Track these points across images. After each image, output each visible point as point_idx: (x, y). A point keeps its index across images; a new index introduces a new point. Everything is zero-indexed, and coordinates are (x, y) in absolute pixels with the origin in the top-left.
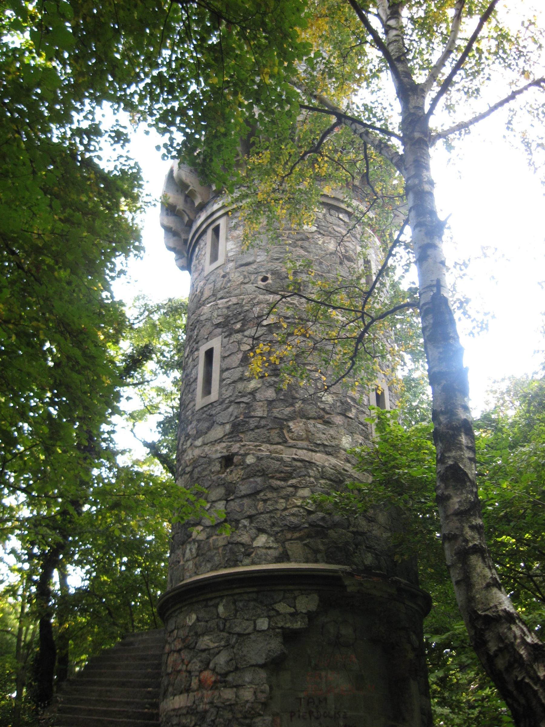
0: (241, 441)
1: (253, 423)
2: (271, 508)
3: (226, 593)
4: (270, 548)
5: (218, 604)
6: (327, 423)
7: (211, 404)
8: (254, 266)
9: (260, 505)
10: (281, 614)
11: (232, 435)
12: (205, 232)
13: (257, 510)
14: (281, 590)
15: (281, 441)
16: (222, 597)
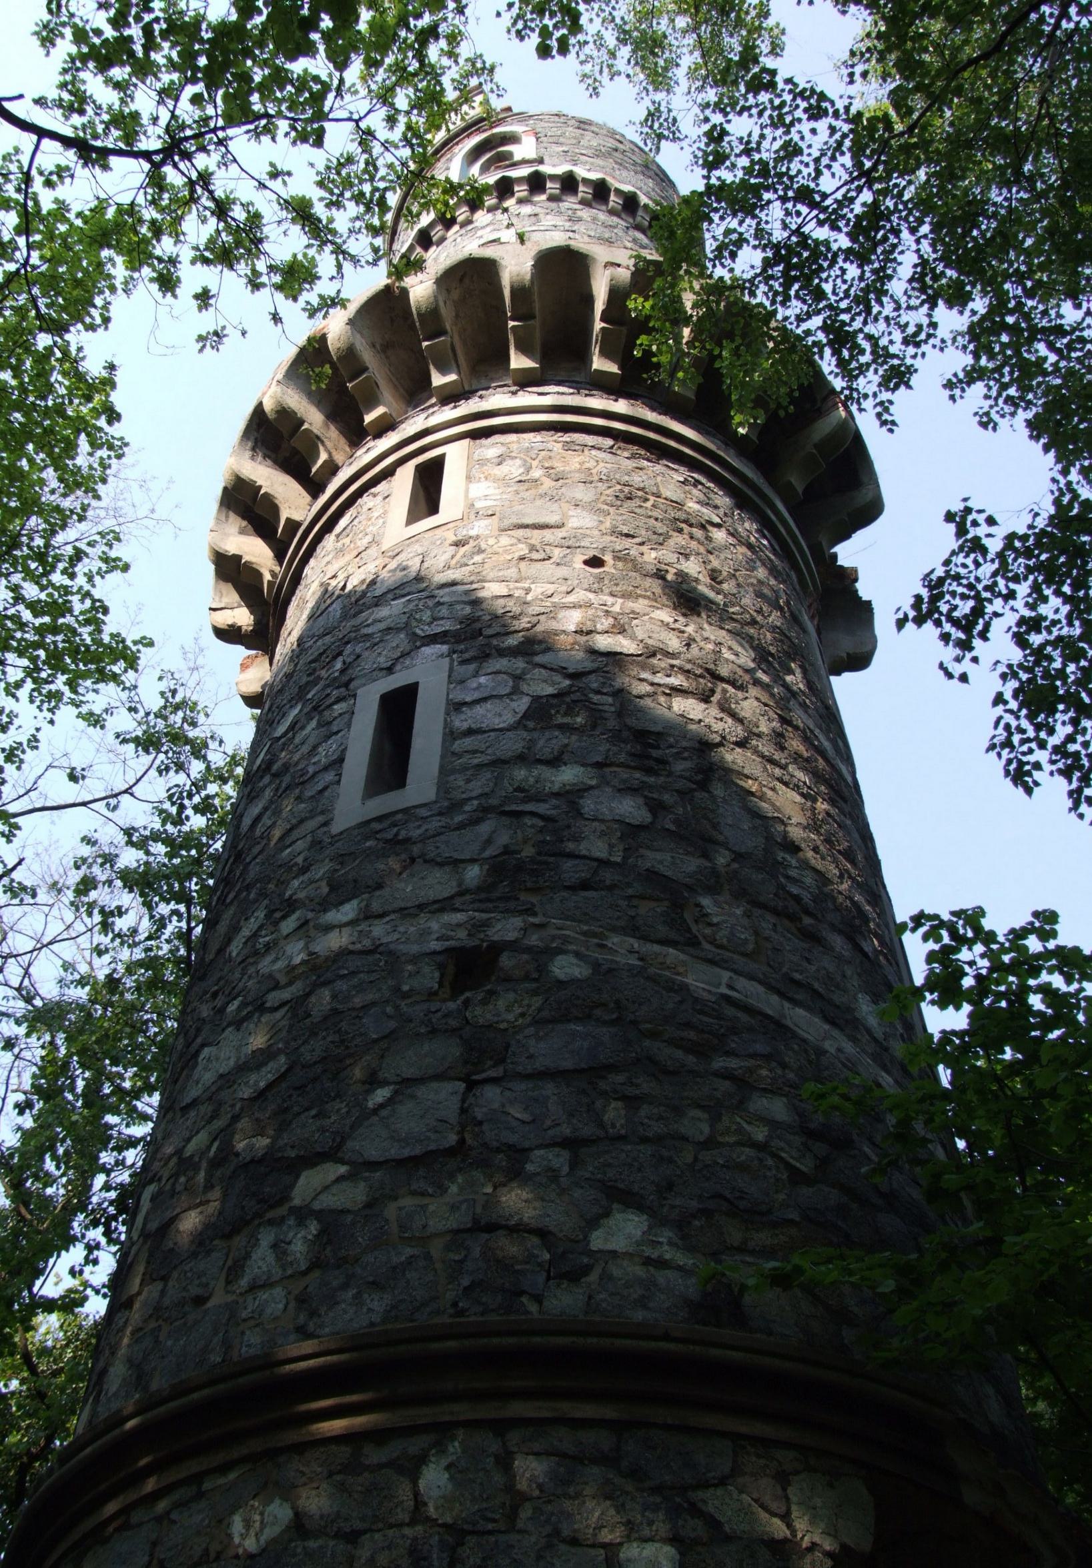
0: (530, 911)
1: (571, 871)
2: (657, 1128)
3: (463, 1411)
4: (661, 1264)
5: (421, 1460)
6: (812, 937)
7: (405, 811)
8: (560, 533)
9: (614, 1113)
10: (728, 1539)
11: (483, 896)
12: (389, 473)
13: (601, 1125)
14: (723, 1434)
15: (673, 935)
16: (442, 1431)
